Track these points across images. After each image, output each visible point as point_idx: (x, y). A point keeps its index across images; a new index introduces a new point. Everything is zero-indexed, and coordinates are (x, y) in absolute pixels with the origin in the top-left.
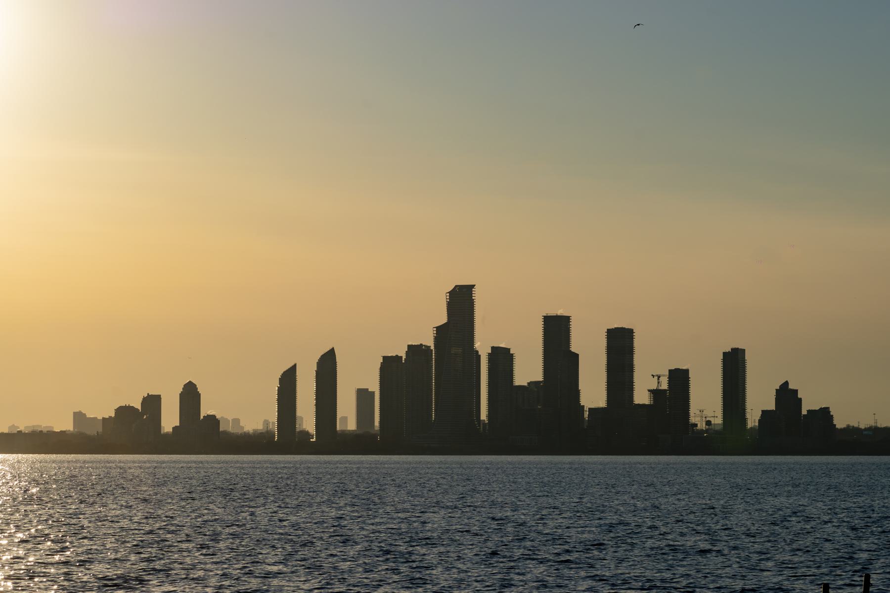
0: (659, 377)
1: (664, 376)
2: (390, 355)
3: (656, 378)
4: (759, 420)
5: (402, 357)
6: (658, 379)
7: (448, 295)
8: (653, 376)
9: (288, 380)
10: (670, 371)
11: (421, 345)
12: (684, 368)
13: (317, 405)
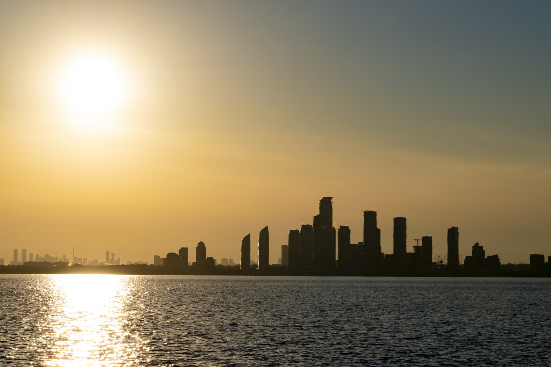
0: (418, 240)
1: (420, 239)
2: (293, 229)
3: (417, 240)
4: (465, 261)
5: (299, 231)
6: (418, 241)
7: (320, 201)
8: (415, 240)
9: (246, 241)
10: (423, 238)
11: (308, 225)
12: (429, 236)
13: (259, 252)
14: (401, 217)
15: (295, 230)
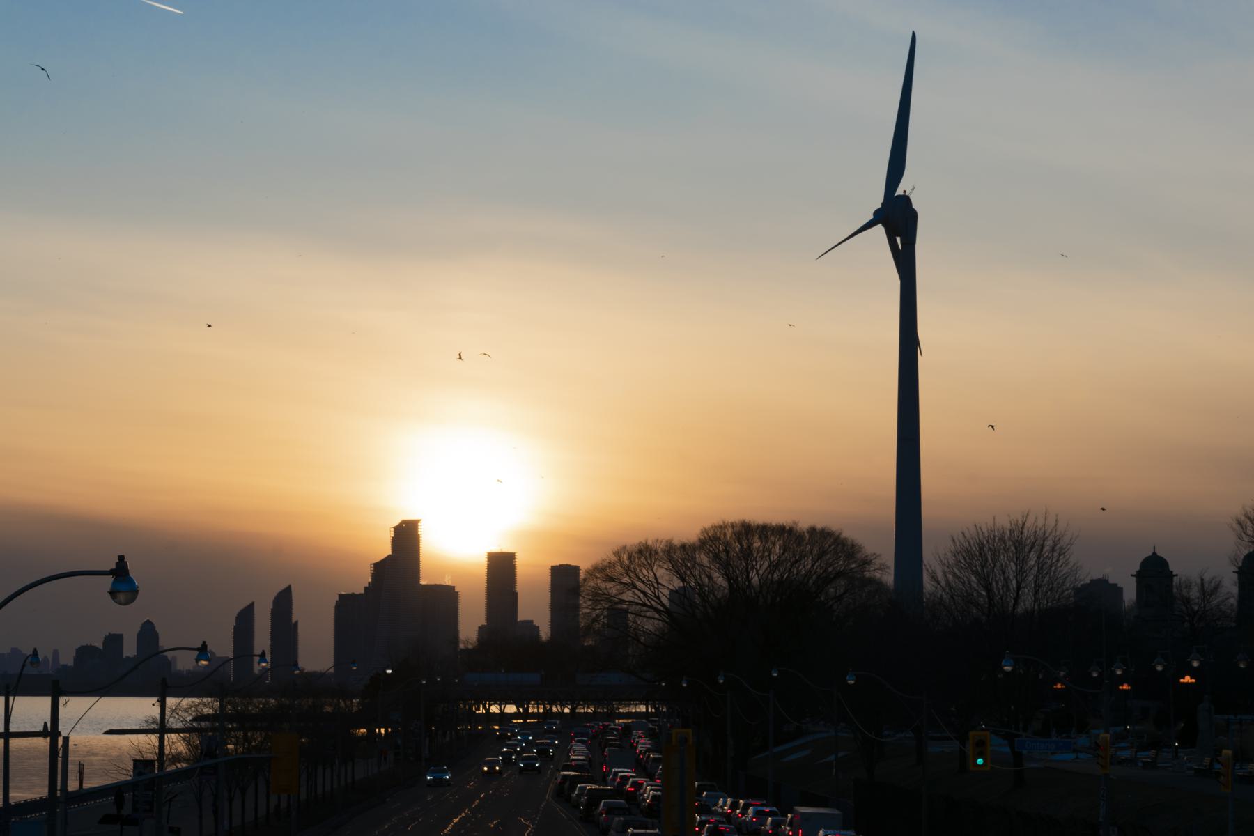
2: (343, 593)
7: (393, 529)
9: (245, 618)
14: (567, 565)
15: (350, 593)
